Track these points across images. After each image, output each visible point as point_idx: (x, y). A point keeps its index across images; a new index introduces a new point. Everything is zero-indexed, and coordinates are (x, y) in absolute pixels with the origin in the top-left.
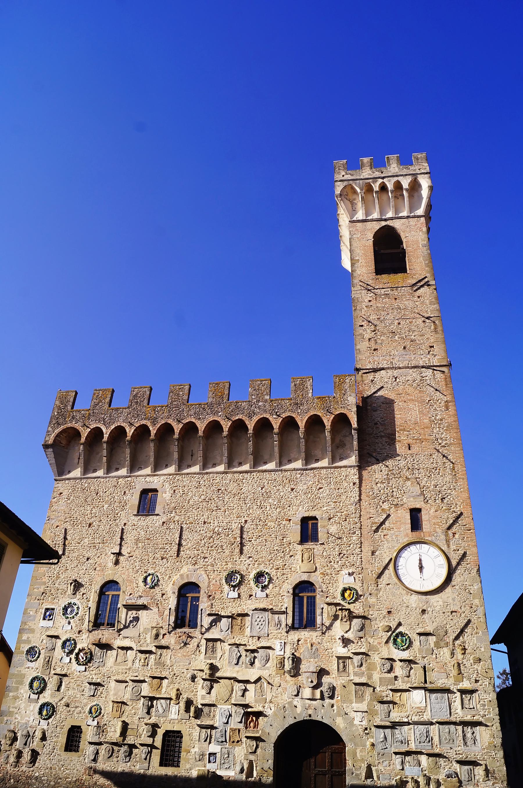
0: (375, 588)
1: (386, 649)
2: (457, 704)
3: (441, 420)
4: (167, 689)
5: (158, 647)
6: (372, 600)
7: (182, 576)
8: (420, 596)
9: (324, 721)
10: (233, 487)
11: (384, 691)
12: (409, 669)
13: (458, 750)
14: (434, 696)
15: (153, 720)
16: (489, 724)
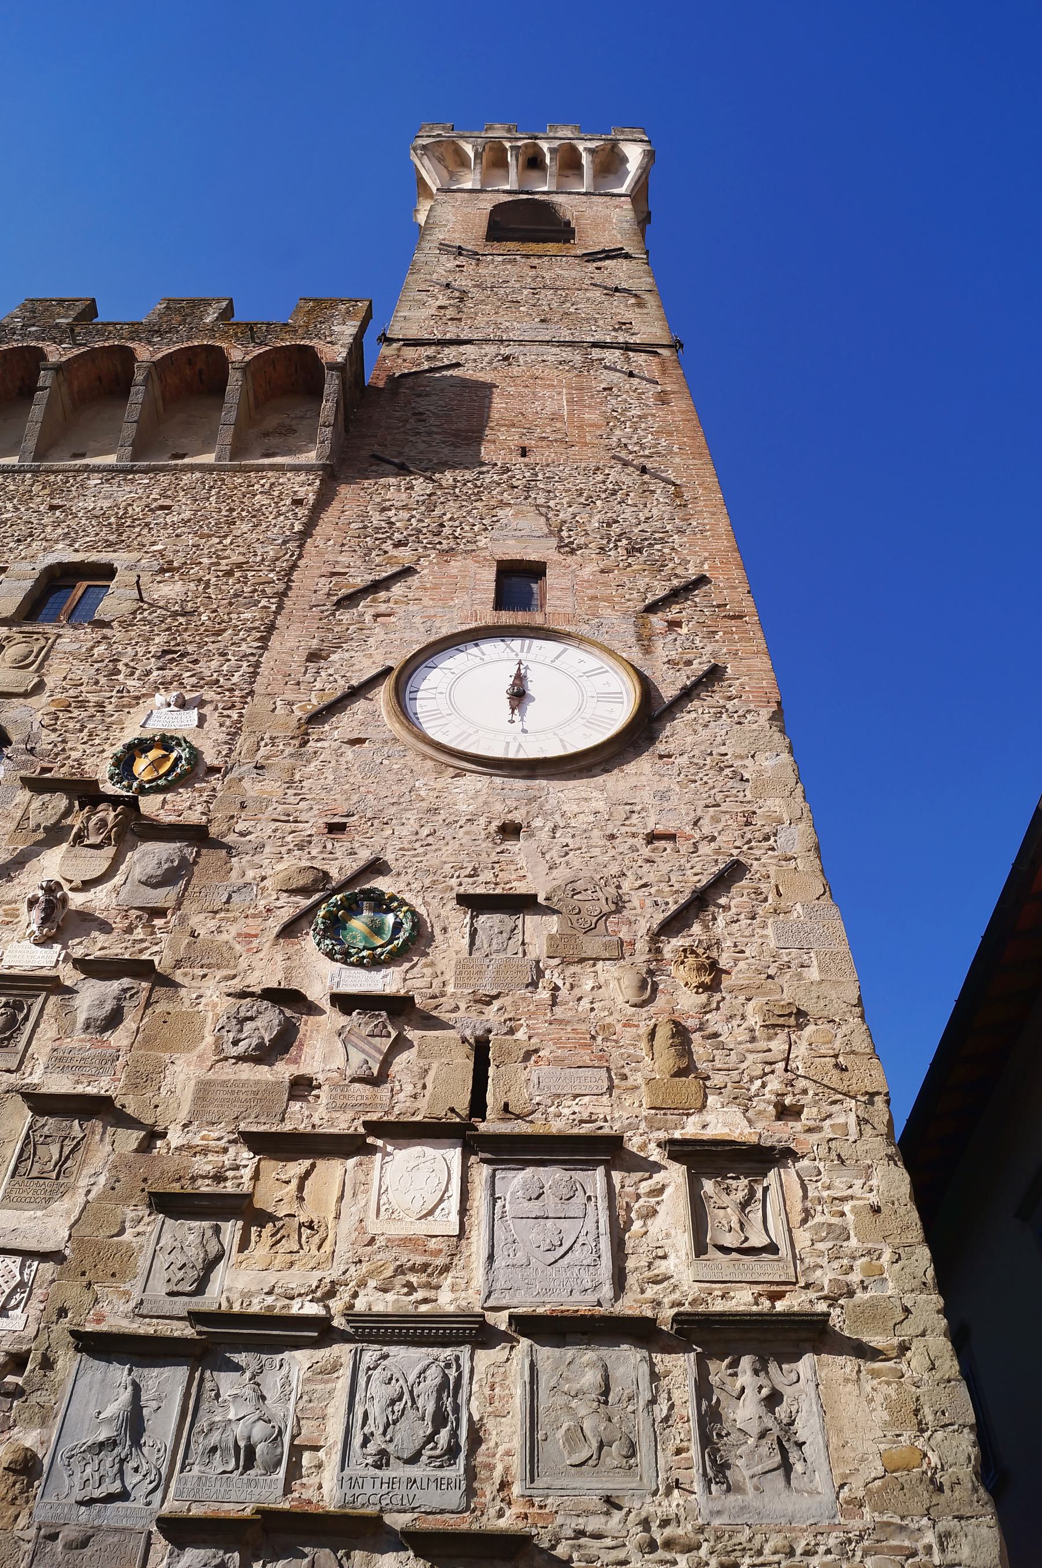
0: (289, 750)
1: (279, 957)
2: (666, 1224)
8: (498, 780)
11: (205, 1151)
12: (385, 1044)
14: (516, 1182)
16: (877, 1341)
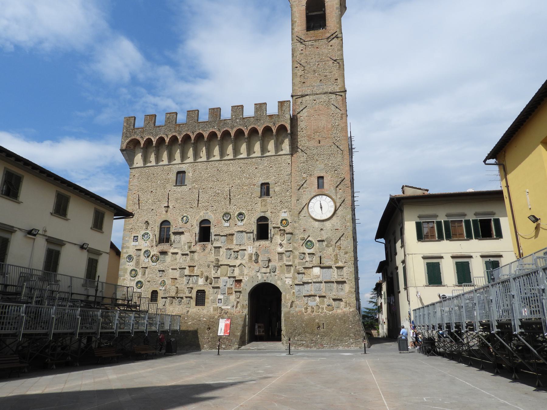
3: (338, 125)
4: (196, 271)
5: (191, 252)
6: (296, 225)
7: (201, 216)
9: (272, 283)
10: (225, 168)
13: (334, 294)
15: (191, 286)
